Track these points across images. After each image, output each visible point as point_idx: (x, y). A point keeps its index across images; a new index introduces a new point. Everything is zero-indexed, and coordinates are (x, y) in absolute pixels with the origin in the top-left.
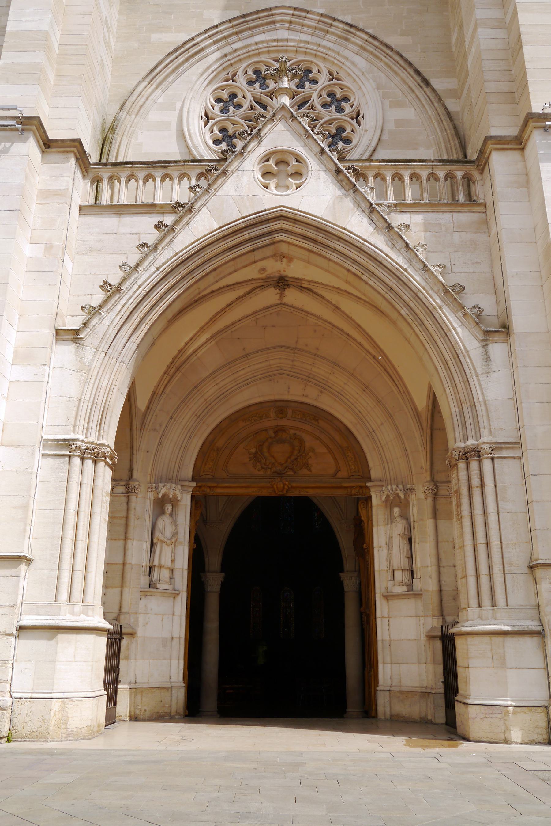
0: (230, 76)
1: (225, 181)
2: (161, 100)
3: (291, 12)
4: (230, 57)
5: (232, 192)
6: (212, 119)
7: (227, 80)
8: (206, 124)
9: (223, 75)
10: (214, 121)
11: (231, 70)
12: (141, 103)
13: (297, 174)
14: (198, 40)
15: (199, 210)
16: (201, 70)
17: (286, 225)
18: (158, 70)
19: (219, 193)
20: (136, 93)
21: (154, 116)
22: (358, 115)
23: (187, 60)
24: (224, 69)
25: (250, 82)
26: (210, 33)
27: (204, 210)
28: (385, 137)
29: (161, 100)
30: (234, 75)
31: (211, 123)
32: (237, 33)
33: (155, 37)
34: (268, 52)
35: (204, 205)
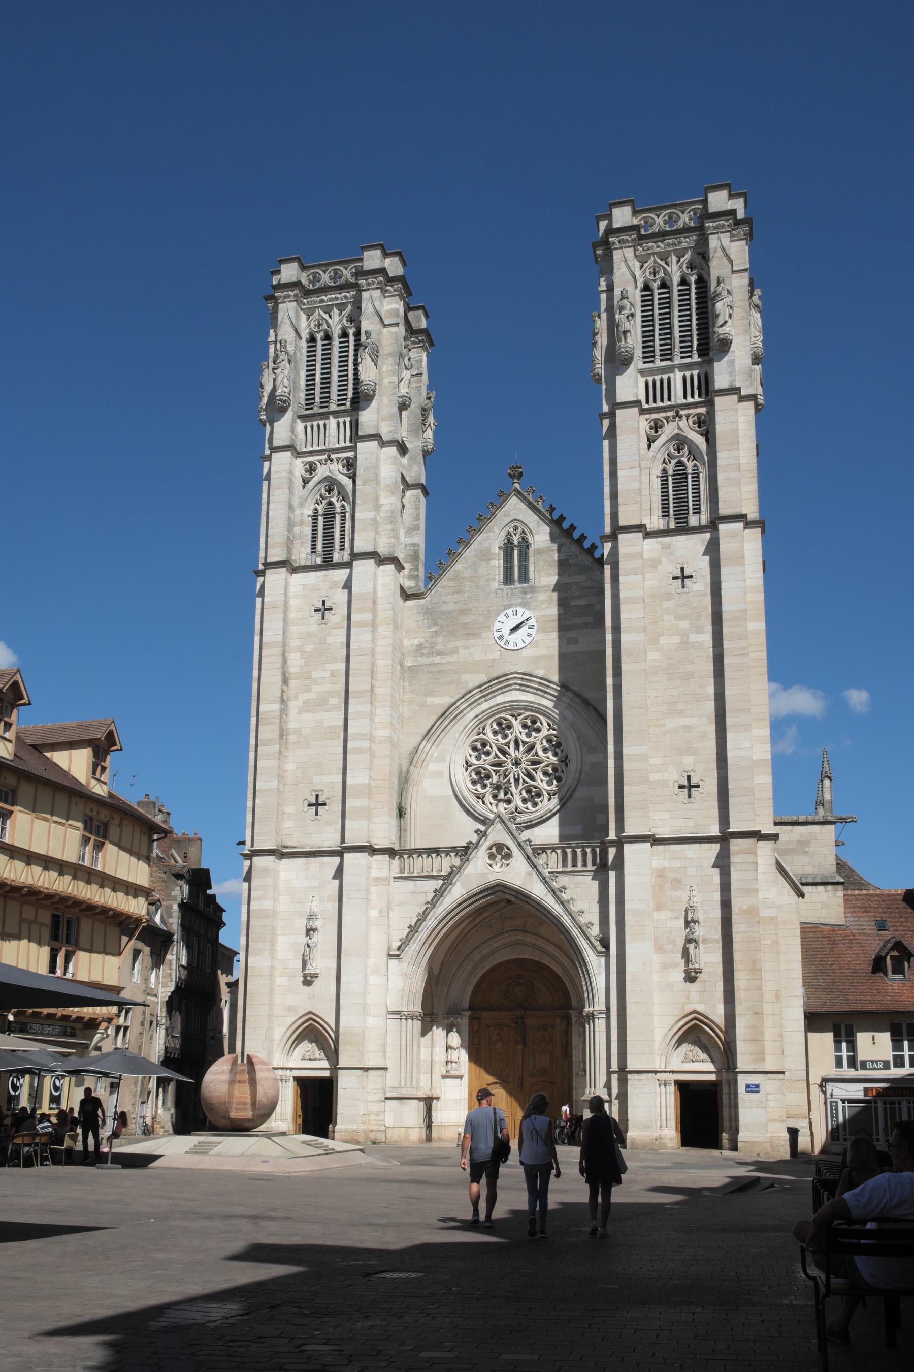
0: (481, 730)
1: (468, 864)
2: (436, 754)
3: (520, 676)
4: (480, 717)
5: (472, 871)
6: (470, 766)
7: (479, 734)
8: (466, 770)
9: (475, 731)
10: (472, 768)
11: (482, 725)
12: (422, 759)
13: (508, 856)
14: (458, 704)
15: (455, 883)
16: (462, 728)
17: (501, 888)
18: (432, 731)
19: (466, 872)
20: (419, 751)
21: (433, 767)
22: (567, 757)
23: (451, 721)
24: (477, 726)
25: (495, 733)
26: (466, 698)
27: (458, 883)
28: (583, 777)
29: (436, 754)
30: (484, 729)
31: (470, 769)
32: (484, 696)
33: (429, 700)
34: (506, 710)
35: (457, 880)
